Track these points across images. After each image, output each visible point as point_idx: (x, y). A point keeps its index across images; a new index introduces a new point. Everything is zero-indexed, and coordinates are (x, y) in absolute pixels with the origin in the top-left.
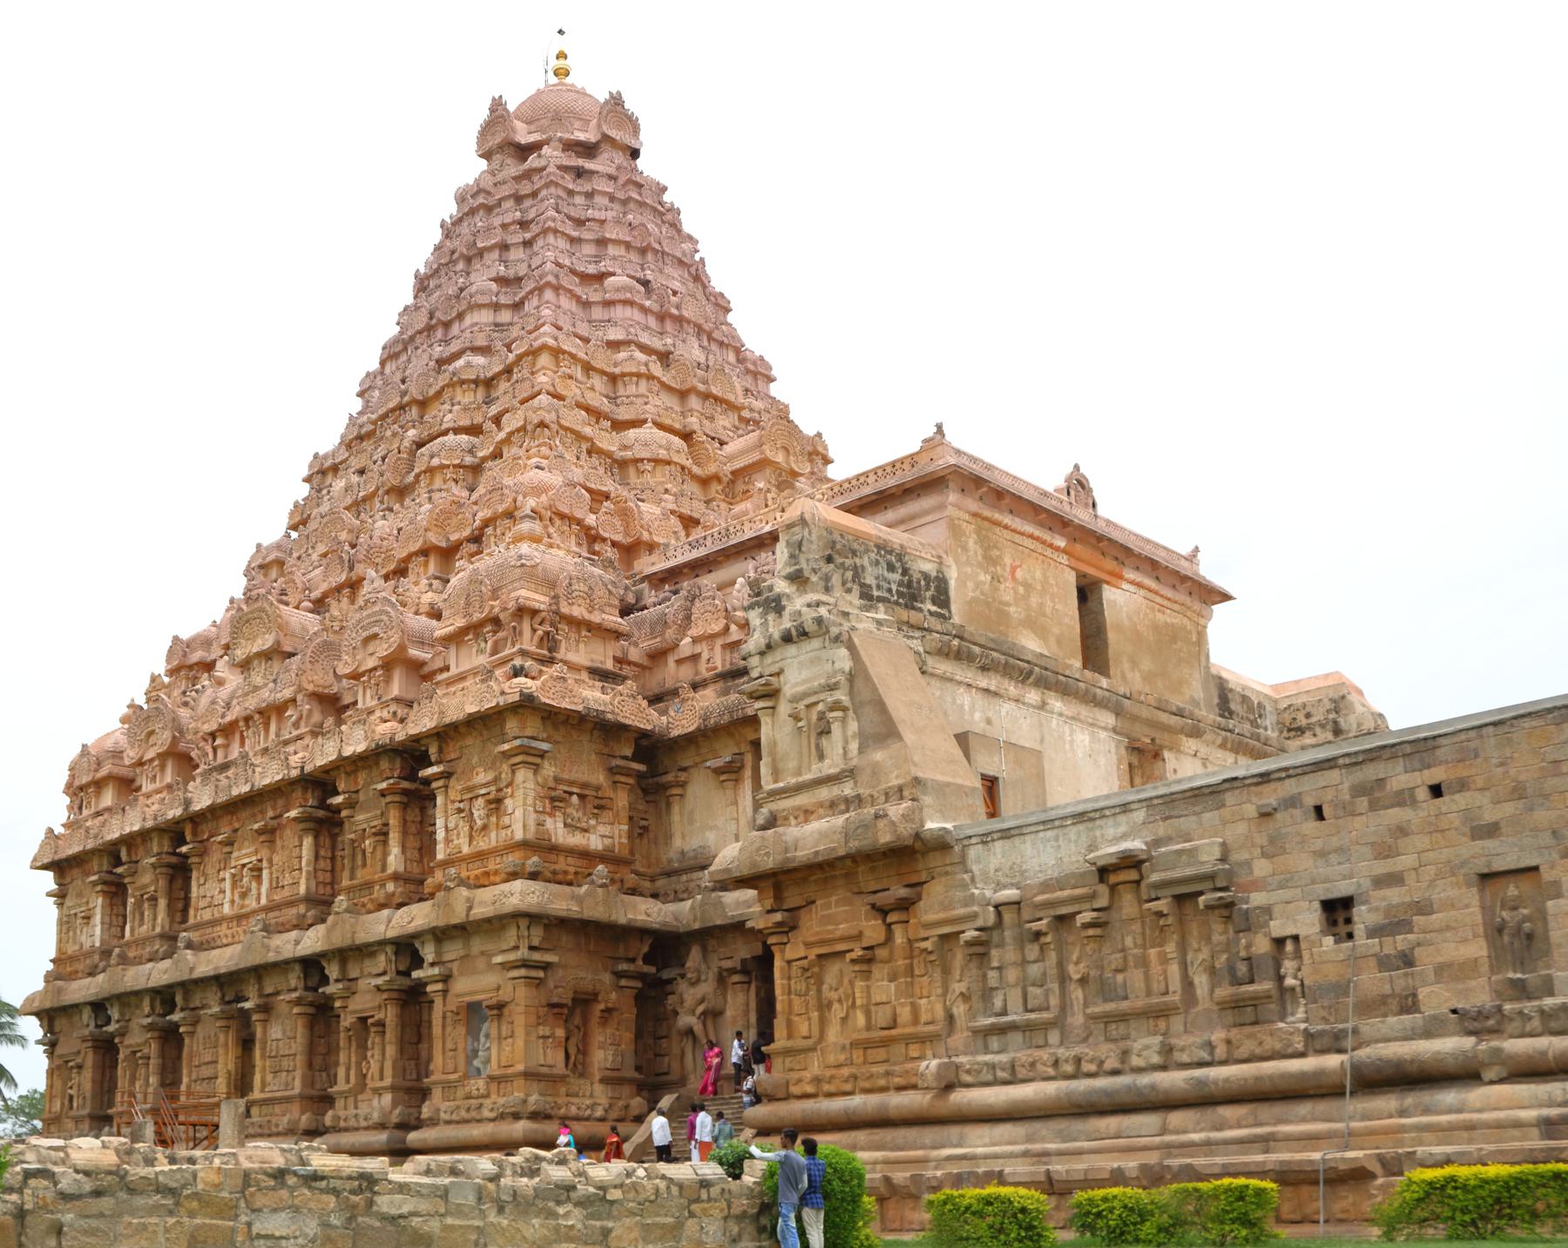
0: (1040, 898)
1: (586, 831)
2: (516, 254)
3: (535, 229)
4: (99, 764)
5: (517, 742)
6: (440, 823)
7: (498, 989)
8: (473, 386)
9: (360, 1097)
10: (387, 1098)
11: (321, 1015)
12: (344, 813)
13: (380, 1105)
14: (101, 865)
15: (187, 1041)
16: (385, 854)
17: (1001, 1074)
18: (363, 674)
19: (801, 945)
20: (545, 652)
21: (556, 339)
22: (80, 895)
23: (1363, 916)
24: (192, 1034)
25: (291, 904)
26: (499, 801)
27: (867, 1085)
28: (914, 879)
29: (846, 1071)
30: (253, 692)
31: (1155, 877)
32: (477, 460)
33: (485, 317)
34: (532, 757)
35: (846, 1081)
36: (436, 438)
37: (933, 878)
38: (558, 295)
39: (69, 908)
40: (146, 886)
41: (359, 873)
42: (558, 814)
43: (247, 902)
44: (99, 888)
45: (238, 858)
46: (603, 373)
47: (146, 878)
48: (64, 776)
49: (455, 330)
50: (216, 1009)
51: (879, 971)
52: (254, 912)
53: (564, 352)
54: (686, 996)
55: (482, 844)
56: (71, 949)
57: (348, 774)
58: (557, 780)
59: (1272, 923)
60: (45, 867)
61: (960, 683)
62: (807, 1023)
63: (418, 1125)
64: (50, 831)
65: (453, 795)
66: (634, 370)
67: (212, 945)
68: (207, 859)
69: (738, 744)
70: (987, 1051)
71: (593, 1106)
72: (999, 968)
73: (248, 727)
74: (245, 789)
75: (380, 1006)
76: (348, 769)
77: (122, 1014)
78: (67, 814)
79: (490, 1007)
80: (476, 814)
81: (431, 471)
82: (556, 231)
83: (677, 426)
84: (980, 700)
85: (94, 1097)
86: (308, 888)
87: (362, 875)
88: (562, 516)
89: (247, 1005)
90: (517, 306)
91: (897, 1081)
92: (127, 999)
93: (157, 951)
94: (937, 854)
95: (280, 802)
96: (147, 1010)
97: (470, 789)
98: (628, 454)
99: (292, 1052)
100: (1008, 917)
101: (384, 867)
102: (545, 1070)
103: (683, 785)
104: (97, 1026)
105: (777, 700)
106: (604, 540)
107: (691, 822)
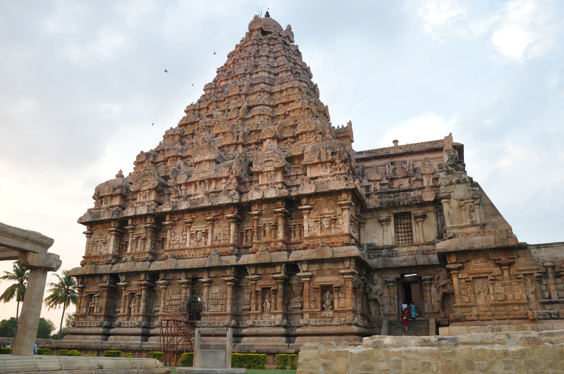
2: (271, 60)
3: (278, 54)
4: (114, 189)
9: (263, 315)
14: (115, 225)
15: (163, 291)
17: (553, 316)
18: (264, 172)
19: (466, 274)
22: (101, 234)
25: (225, 246)
26: (336, 220)
27: (499, 318)
28: (511, 257)
29: (490, 313)
30: (202, 173)
32: (274, 115)
33: (266, 74)
35: (490, 316)
37: (519, 257)
40: (141, 234)
43: (199, 244)
44: (114, 233)
45: (196, 228)
48: (93, 192)
49: (254, 76)
50: (184, 280)
51: (498, 284)
52: (204, 248)
54: (373, 289)
55: (328, 233)
56: (94, 254)
57: (258, 205)
60: (84, 224)
62: (468, 298)
65: (311, 216)
67: (181, 257)
68: (175, 227)
69: (389, 214)
70: (545, 309)
72: (546, 285)
73: (200, 184)
74: (210, 204)
75: (275, 285)
76: (259, 203)
77: (126, 279)
79: (335, 287)
80: (324, 223)
81: (260, 115)
85: (106, 308)
87: (264, 239)
91: (511, 317)
93: (148, 258)
94: (522, 250)
95: (219, 212)
97: (321, 215)
99: (225, 297)
100: (550, 270)
101: (276, 237)
103: (364, 223)
104: (110, 283)
105: (450, 200)
107: (367, 235)
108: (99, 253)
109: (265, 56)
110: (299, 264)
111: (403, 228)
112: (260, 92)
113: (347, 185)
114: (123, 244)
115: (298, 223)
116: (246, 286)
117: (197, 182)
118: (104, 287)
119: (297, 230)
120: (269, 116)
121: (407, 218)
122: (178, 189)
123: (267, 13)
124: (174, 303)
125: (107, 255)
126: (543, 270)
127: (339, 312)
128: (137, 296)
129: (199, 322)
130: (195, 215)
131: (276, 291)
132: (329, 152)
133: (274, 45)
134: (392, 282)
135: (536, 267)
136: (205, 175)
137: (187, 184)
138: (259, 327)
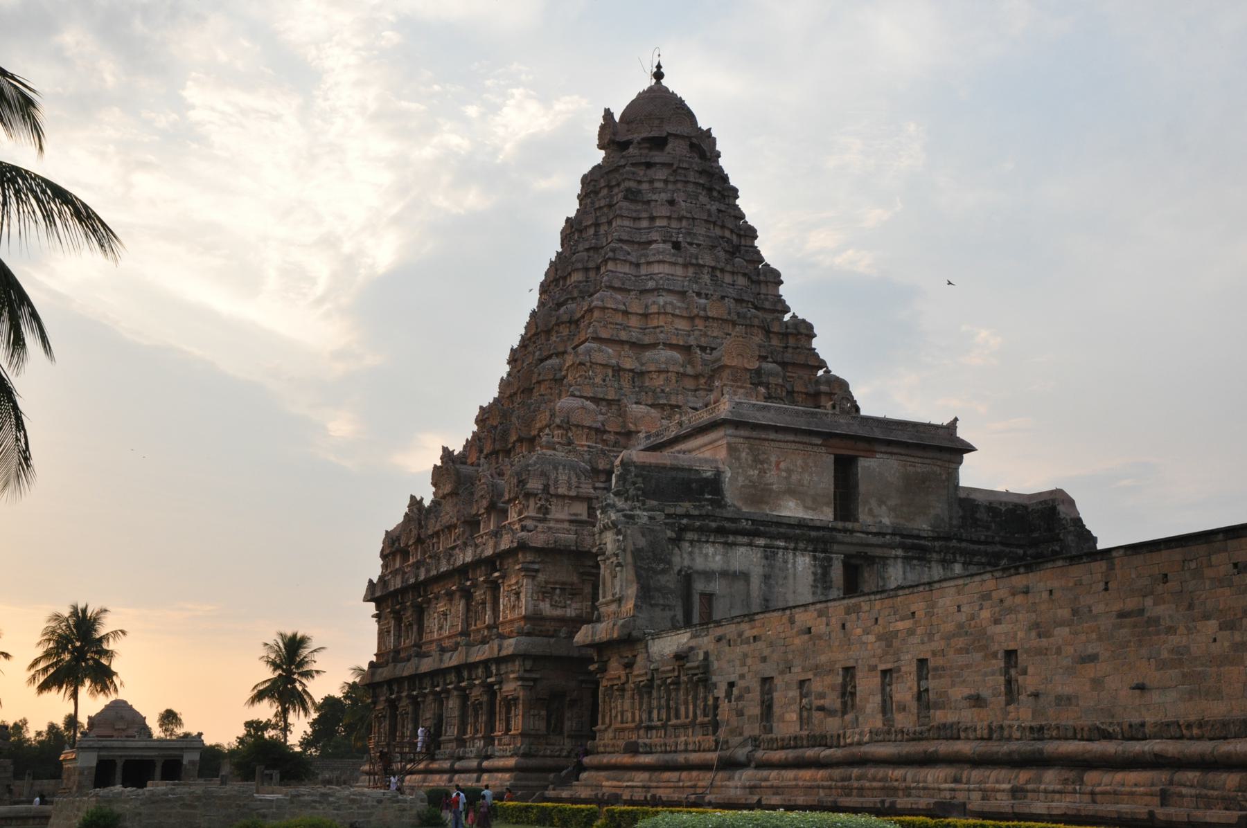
0: (662, 669)
1: (565, 607)
2: (602, 230)
5: (520, 566)
6: (501, 600)
7: (515, 690)
8: (568, 325)
10: (482, 742)
11: (464, 698)
12: (472, 590)
13: (480, 744)
15: (422, 706)
16: (485, 614)
18: (480, 515)
20: (541, 516)
21: (603, 301)
22: (386, 619)
23: (735, 691)
24: (424, 702)
25: (455, 636)
31: (688, 665)
34: (530, 573)
36: (546, 359)
38: (616, 264)
39: (383, 625)
41: (478, 622)
42: (547, 600)
46: (637, 314)
47: (409, 613)
49: (568, 283)
51: (628, 694)
53: (608, 308)
58: (546, 582)
59: (715, 691)
61: (707, 542)
63: (488, 757)
64: (371, 581)
66: (656, 311)
71: (561, 750)
78: (380, 570)
81: (539, 382)
82: (622, 216)
83: (681, 343)
84: (720, 548)
86: (462, 628)
88: (577, 426)
89: (438, 689)
90: (598, 268)
92: (399, 681)
96: (406, 688)
97: (510, 586)
98: (644, 368)
102: (533, 732)
106: (610, 432)
109: (592, 224)
112: (558, 324)
113: (512, 542)
123: (659, 67)
124: (428, 724)
126: (649, 677)
129: (437, 752)
131: (481, 704)
132: (515, 481)
133: (618, 185)
135: (643, 672)
137: (437, 534)
138: (469, 758)
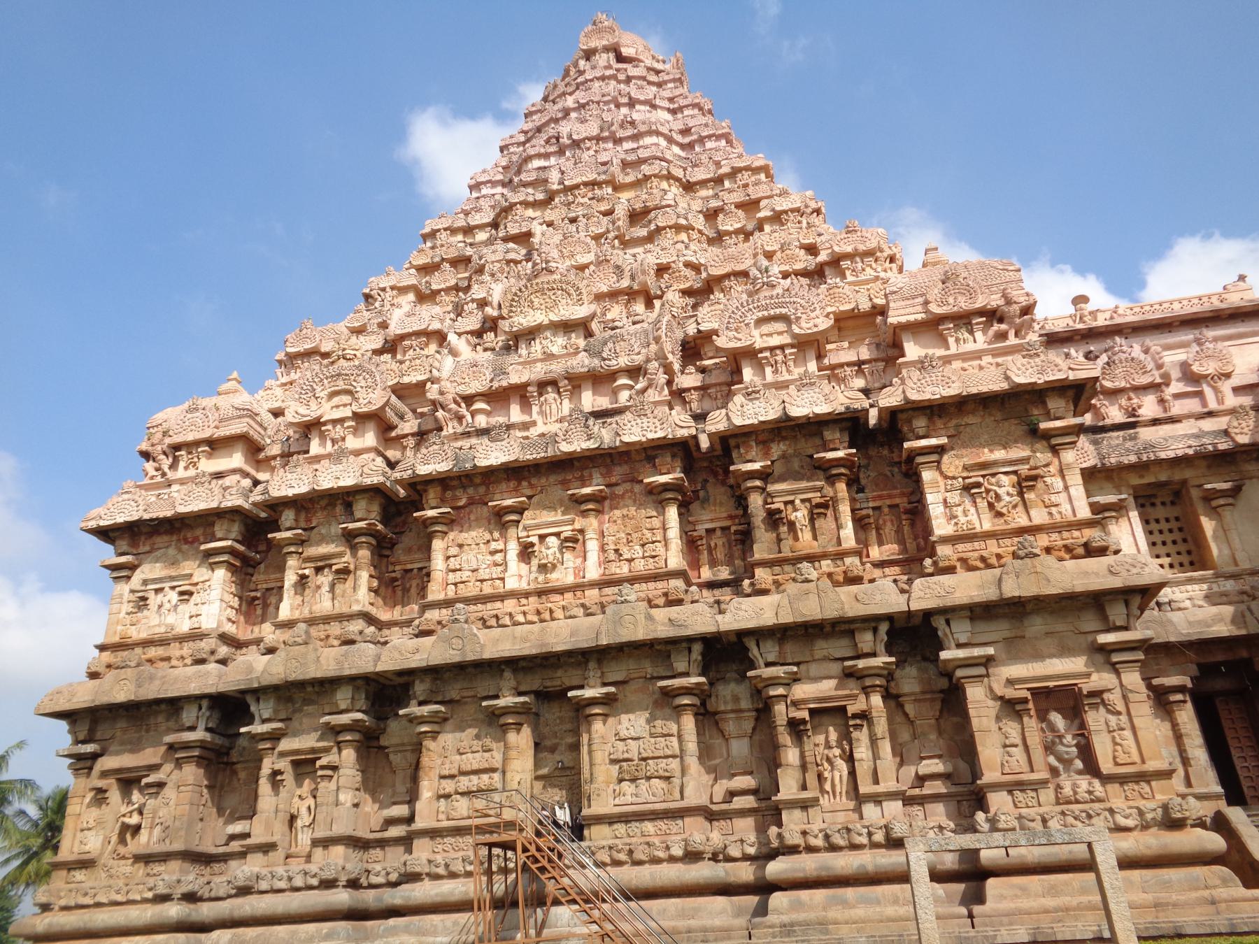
30: (542, 360)
45: (538, 526)
74: (591, 444)
108: (162, 630)
110: (939, 623)
111: (1156, 533)
114: (255, 598)
115: (888, 502)
116: (733, 711)
117: (529, 389)
118: (186, 746)
119: (889, 524)
120: (700, 232)
121: (1163, 504)
122: (463, 410)
125: (196, 635)
127: (1122, 780)
128: (322, 768)
130: (531, 486)
134: (1181, 689)
136: (557, 368)
